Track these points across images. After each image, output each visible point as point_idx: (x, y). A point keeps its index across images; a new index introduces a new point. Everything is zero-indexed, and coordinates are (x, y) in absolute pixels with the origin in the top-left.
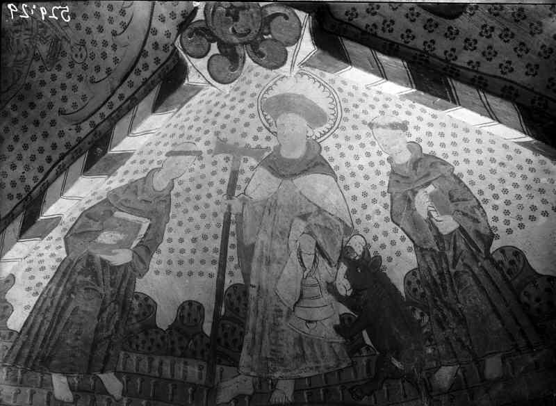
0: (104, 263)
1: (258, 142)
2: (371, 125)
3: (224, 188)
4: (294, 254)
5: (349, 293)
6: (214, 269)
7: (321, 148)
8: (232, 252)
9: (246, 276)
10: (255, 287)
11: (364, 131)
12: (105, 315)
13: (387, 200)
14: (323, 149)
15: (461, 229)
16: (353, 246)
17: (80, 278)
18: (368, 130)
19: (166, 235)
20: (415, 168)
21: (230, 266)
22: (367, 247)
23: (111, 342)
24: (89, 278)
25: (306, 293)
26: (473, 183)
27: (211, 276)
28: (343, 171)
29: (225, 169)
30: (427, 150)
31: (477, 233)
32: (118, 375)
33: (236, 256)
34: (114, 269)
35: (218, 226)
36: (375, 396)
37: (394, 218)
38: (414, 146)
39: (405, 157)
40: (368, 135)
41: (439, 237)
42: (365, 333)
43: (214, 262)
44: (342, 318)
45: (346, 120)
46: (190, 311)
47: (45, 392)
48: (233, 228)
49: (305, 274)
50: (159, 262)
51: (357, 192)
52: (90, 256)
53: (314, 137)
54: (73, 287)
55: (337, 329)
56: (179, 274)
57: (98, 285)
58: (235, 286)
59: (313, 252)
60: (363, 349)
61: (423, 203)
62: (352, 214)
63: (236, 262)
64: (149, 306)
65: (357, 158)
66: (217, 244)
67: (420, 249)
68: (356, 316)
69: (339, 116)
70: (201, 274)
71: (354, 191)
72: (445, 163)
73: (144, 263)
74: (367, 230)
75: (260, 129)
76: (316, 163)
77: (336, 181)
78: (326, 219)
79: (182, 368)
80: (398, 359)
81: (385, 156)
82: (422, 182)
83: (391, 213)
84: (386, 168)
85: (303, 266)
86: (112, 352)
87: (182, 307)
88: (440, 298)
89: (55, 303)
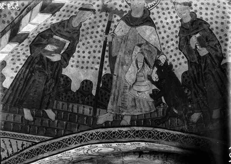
1: (122, 8)
3: (105, 29)
4: (134, 62)
5: (157, 80)
6: (98, 66)
7: (150, 13)
8: (106, 59)
9: (112, 70)
12: (48, 84)
13: (178, 39)
14: (151, 13)
15: (209, 54)
16: (161, 60)
19: (77, 49)
20: (192, 25)
21: (106, 65)
22: (167, 60)
23: (50, 96)
24: (41, 66)
25: (139, 79)
26: (217, 33)
27: (96, 69)
28: (159, 25)
29: (105, 20)
30: (199, 16)
31: (216, 56)
32: (53, 110)
33: (108, 61)
34: (53, 63)
35: (101, 46)
36: (165, 124)
37: (180, 48)
38: (193, 14)
39: (188, 19)
41: (199, 57)
42: (163, 98)
43: (98, 63)
44: (153, 91)
46: (86, 84)
47: (20, 117)
48: (107, 48)
49: (138, 71)
50: (73, 61)
51: (165, 35)
52: (41, 56)
53: (147, 8)
55: (151, 96)
56: (82, 68)
57: (45, 70)
58: (107, 75)
59: (143, 62)
60: (162, 104)
61: (194, 41)
62: (161, 45)
63: (108, 64)
64: (68, 81)
65: (166, 19)
66: (100, 55)
68: (160, 90)
70: (92, 68)
71: (163, 35)
72: (206, 23)
73: (66, 62)
74: (167, 53)
77: (156, 29)
78: (149, 47)
79: (82, 109)
80: (176, 109)
81: (179, 19)
82: (195, 31)
83: (179, 45)
84: (179, 25)
85: (138, 67)
86: (51, 101)
87: (83, 83)
88: (197, 84)
89: (25, 77)
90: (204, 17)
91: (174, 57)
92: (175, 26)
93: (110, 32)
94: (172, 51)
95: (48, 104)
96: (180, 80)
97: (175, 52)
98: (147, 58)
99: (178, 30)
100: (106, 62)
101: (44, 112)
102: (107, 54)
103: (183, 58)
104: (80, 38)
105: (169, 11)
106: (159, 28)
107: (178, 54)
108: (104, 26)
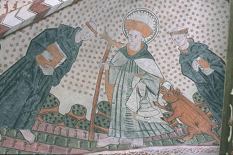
0: (39, 70)
1: (120, 40)
2: (171, 34)
3: (102, 57)
4: (135, 91)
5: (166, 105)
6: (93, 92)
7: (148, 46)
9: (110, 97)
10: (114, 103)
11: (168, 36)
12: (30, 100)
13: (179, 66)
17: (25, 73)
18: (170, 36)
19: (72, 69)
21: (101, 93)
23: (31, 114)
25: (143, 106)
26: (217, 51)
27: (91, 95)
28: (158, 57)
29: (104, 48)
30: (196, 41)
32: (33, 132)
34: (42, 74)
35: (97, 73)
37: (183, 73)
39: (188, 45)
40: (170, 39)
41: (205, 76)
43: (93, 89)
45: (160, 32)
46: (78, 109)
48: (103, 76)
50: (66, 81)
51: (165, 65)
53: (145, 42)
54: (20, 77)
57: (32, 82)
58: (104, 102)
59: (145, 89)
61: (196, 66)
65: (164, 50)
67: (198, 84)
69: (158, 30)
71: (163, 64)
72: (203, 45)
73: (58, 79)
75: (122, 34)
76: (145, 53)
81: (178, 47)
82: (196, 56)
85: (140, 95)
86: (30, 120)
87: (74, 107)
88: (212, 101)
90: (201, 41)
91: (178, 83)
92: (174, 56)
93: (107, 60)
94: (175, 77)
95: (27, 122)
96: (192, 101)
97: (179, 77)
98: (150, 87)
99: (178, 58)
100: (102, 89)
101: (18, 132)
102: (103, 81)
103: (189, 81)
104: (78, 58)
105: (166, 42)
106: (157, 60)
107: (183, 79)
108: (102, 53)
